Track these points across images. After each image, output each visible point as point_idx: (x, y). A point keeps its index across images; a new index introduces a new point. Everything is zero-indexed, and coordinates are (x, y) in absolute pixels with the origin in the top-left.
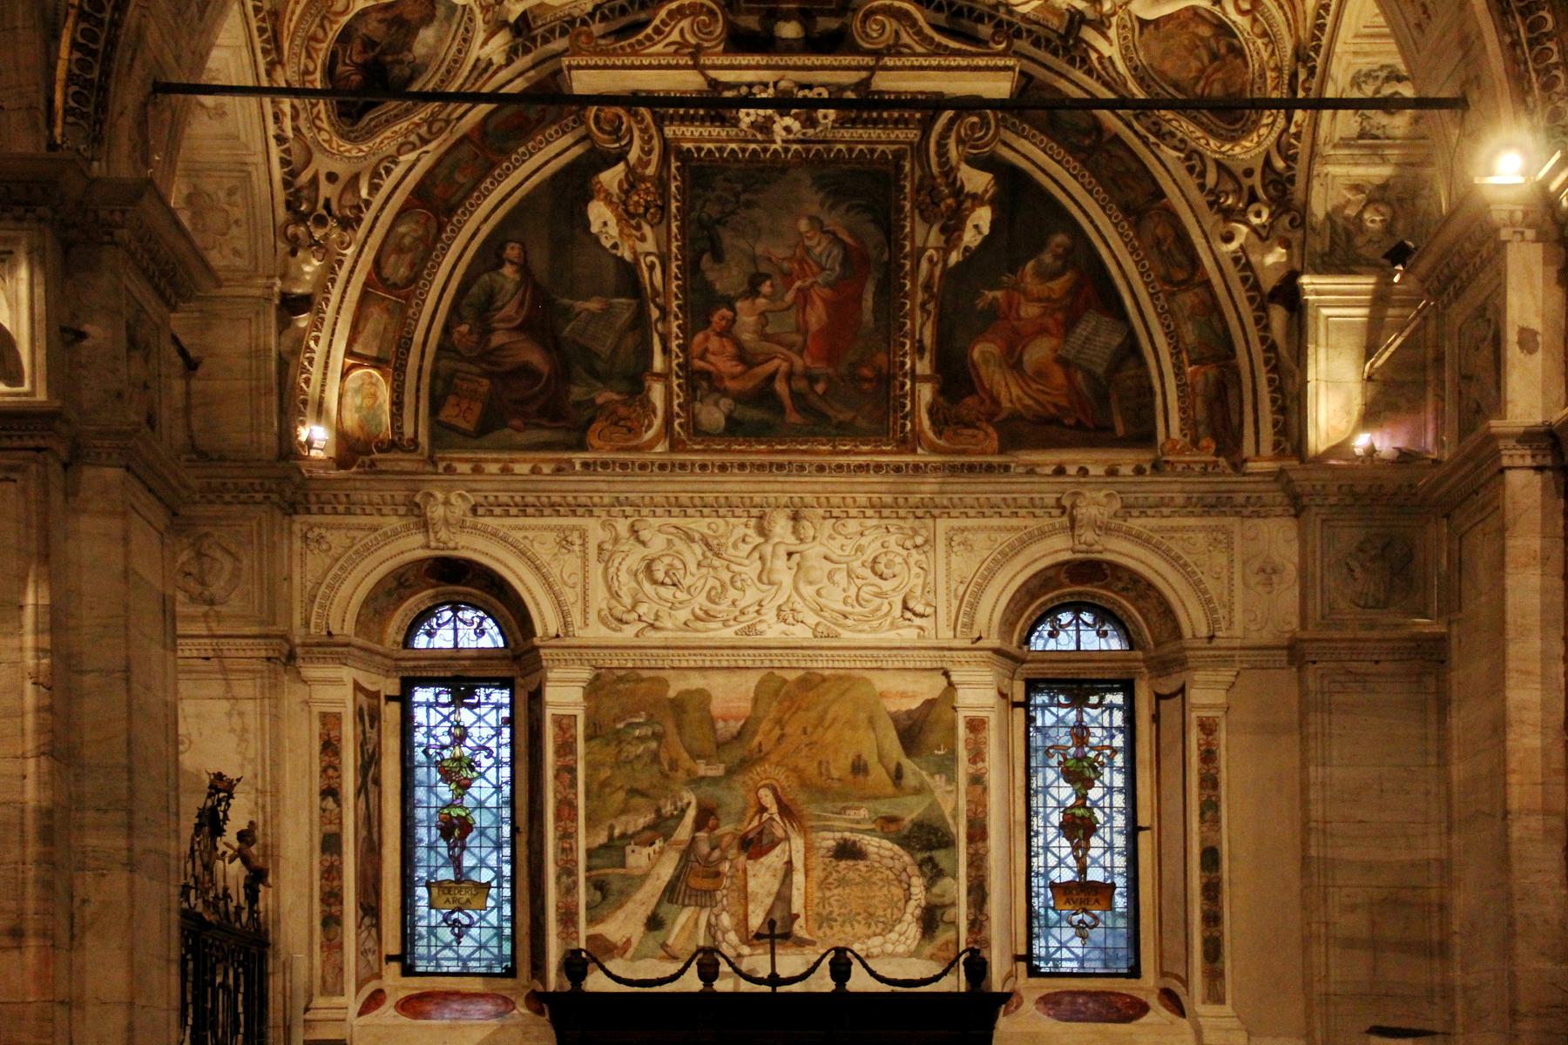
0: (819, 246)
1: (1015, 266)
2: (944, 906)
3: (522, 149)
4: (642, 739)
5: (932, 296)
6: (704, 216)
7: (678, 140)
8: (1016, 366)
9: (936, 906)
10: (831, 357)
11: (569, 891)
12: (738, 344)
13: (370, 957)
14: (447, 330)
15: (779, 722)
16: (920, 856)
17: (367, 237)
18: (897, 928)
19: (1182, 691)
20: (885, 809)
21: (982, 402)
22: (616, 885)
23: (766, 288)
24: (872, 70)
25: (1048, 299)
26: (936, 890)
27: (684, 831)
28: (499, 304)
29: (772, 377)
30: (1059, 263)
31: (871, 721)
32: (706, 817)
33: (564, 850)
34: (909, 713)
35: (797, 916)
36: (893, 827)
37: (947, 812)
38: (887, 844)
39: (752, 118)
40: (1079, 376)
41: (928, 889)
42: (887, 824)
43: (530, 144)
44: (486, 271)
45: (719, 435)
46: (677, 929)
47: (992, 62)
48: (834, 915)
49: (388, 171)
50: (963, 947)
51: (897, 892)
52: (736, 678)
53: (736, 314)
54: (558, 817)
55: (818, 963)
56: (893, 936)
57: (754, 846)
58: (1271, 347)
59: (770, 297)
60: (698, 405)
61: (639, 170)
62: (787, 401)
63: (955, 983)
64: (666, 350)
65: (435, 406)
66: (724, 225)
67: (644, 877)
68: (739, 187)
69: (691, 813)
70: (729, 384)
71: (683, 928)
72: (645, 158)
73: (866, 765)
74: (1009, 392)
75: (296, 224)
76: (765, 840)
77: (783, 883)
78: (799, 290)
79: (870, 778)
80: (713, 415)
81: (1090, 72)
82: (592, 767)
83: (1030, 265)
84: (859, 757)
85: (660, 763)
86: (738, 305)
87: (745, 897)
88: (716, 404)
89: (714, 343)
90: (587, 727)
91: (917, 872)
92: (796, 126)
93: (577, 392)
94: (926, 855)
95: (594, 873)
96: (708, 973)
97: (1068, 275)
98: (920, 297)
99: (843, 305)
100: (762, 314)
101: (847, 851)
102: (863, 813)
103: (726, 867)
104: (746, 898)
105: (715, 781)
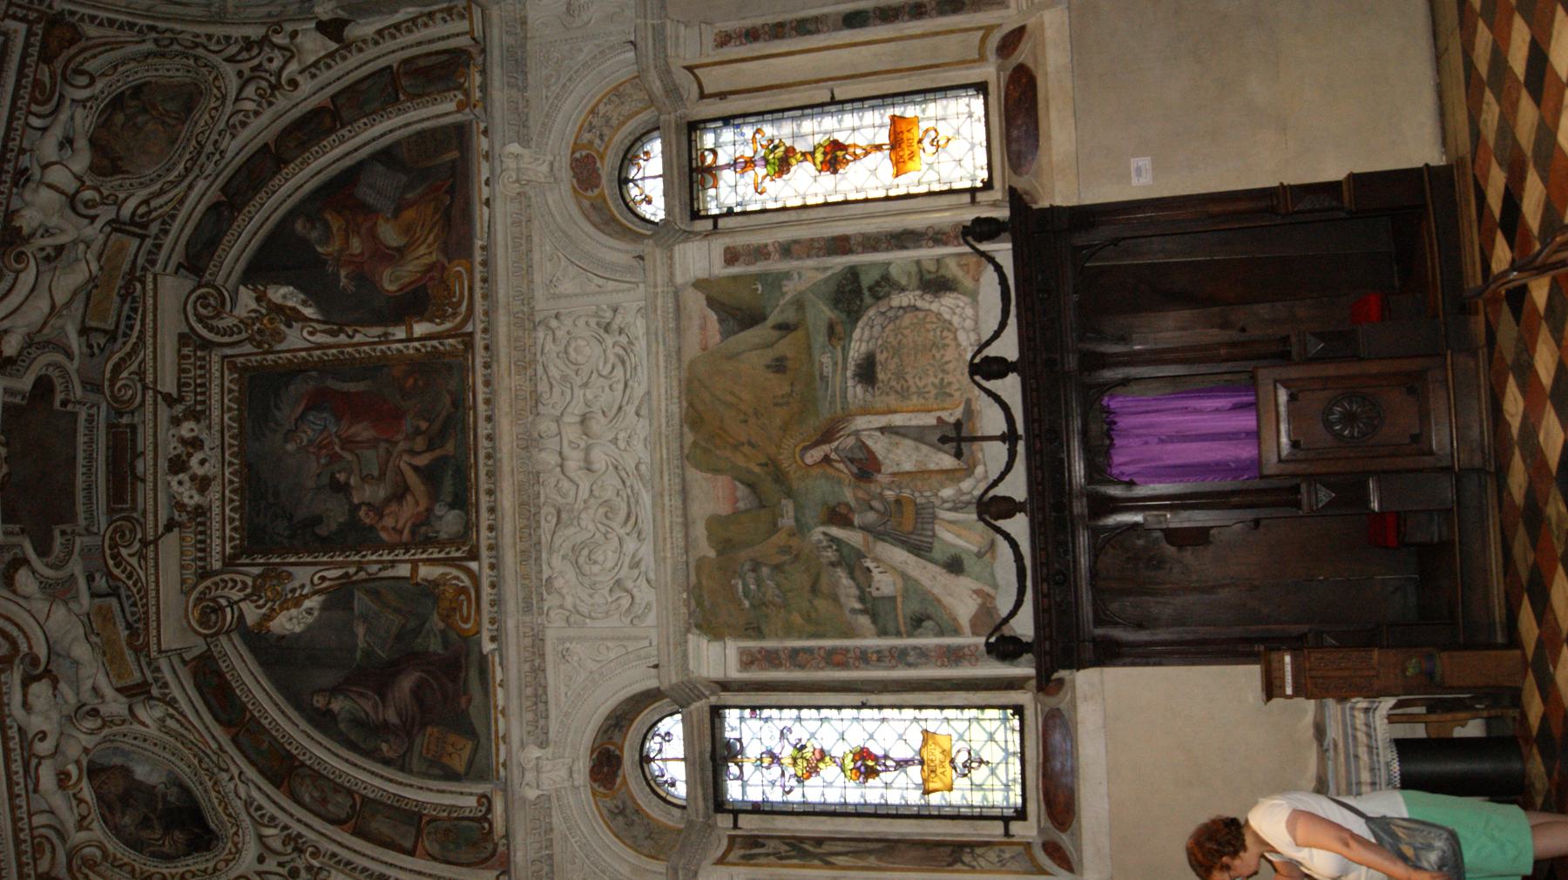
0: (307, 434)
1: (320, 262)
2: (920, 272)
3: (237, 691)
4: (759, 582)
5: (341, 331)
6: (286, 534)
8: (401, 251)
9: (921, 279)
10: (397, 416)
11: (924, 655)
12: (388, 501)
13: (1007, 856)
14: (387, 762)
15: (736, 447)
16: (868, 299)
17: (313, 830)
18: (947, 317)
19: (690, 69)
20: (820, 338)
21: (432, 278)
22: (915, 606)
23: (342, 477)
24: (156, 392)
26: (904, 282)
27: (854, 538)
29: (416, 469)
31: (730, 357)
32: (839, 516)
33: (879, 660)
34: (721, 321)
35: (939, 419)
36: (839, 329)
37: (821, 276)
38: (857, 334)
39: (194, 493)
40: (409, 196)
41: (903, 290)
42: (836, 335)
43: (234, 685)
45: (467, 514)
46: (961, 542)
47: (150, 293)
48: (937, 381)
49: (260, 808)
50: (967, 249)
51: (907, 319)
52: (695, 491)
53: (363, 503)
54: (843, 665)
55: (989, 393)
56: (956, 320)
57: (866, 467)
58: (380, 32)
60: (443, 536)
61: (249, 591)
62: (438, 453)
63: (1003, 250)
64: (393, 563)
65: (451, 776)
66: (292, 516)
67: (905, 576)
69: (835, 531)
70: (421, 508)
71: (959, 536)
72: (239, 586)
73: (777, 360)
74: (424, 255)
76: (860, 455)
77: (904, 436)
78: (342, 449)
79: (789, 354)
80: (449, 522)
81: (173, 217)
82: (789, 631)
83: (320, 249)
84: (768, 367)
85: (784, 563)
86: (356, 501)
87: (923, 473)
88: (440, 518)
89: (389, 522)
90: (749, 637)
91: (885, 301)
92: (198, 456)
93: (435, 645)
94: (866, 293)
95: (903, 629)
96: (1007, 507)
98: (342, 338)
99: (349, 407)
101: (867, 372)
102: (826, 359)
103: (890, 494)
104: (923, 472)
105: (799, 508)
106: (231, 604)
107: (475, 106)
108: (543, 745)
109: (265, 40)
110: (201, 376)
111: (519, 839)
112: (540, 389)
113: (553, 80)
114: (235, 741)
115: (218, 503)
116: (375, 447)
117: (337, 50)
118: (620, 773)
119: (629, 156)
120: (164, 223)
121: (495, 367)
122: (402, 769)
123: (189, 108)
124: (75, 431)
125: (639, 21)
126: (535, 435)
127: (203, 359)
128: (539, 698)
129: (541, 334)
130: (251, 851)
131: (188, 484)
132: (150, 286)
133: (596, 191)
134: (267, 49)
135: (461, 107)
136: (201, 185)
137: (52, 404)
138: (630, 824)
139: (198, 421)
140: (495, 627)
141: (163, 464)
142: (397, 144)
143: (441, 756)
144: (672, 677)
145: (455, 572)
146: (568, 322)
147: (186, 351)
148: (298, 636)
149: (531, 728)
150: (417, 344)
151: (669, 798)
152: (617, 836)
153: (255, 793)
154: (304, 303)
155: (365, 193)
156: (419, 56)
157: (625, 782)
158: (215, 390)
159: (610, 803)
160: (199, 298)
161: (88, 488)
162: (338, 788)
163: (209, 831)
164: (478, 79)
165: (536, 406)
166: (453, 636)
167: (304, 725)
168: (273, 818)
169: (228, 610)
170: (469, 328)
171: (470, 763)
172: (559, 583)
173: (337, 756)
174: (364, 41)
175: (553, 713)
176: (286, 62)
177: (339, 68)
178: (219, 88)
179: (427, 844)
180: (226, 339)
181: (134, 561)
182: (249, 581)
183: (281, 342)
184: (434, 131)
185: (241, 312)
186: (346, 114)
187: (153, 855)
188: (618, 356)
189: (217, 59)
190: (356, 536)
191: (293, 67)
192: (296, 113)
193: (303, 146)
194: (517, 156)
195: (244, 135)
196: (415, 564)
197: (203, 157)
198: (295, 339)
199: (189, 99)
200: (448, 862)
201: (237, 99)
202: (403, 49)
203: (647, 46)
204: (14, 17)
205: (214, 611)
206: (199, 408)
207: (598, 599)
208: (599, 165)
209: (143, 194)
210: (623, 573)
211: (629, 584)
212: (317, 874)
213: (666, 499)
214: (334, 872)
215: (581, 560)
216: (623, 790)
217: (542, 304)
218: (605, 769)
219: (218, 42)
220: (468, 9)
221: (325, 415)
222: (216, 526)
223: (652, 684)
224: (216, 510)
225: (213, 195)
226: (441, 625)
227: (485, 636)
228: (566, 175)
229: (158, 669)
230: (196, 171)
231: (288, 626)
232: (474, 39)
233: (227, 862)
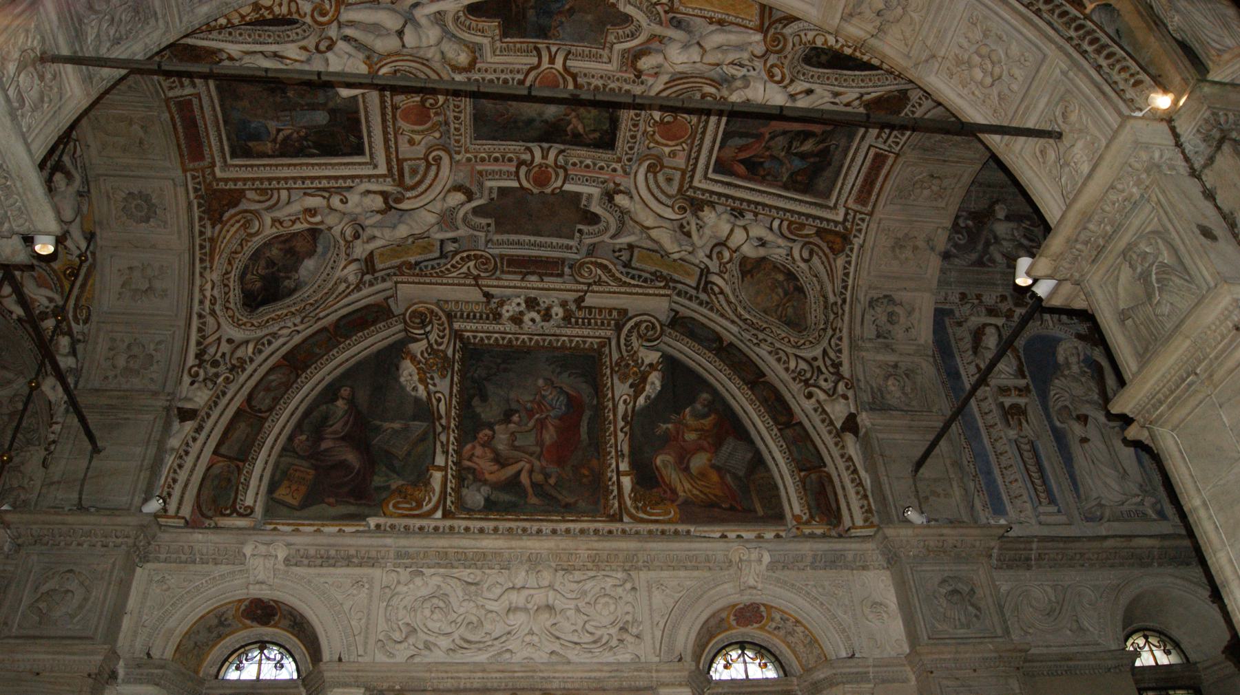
0: (550, 395)
1: (678, 410)
3: (361, 334)
5: (627, 423)
6: (476, 375)
7: (463, 331)
8: (687, 469)
10: (560, 462)
14: (291, 438)
17: (246, 381)
21: (665, 492)
23: (515, 418)
24: (586, 292)
25: (702, 430)
28: (331, 423)
29: (519, 472)
30: (706, 409)
39: (511, 313)
40: (729, 478)
43: (365, 332)
44: (326, 403)
45: (480, 511)
47: (657, 292)
49: (270, 343)
58: (850, 459)
59: (518, 424)
60: (464, 491)
61: (435, 347)
64: (446, 452)
65: (273, 487)
68: (499, 361)
70: (487, 476)
72: (440, 340)
74: (683, 487)
75: (199, 366)
78: (537, 420)
80: (475, 496)
81: (711, 309)
83: (688, 410)
86: (496, 427)
88: (479, 490)
89: (479, 451)
92: (538, 318)
93: (378, 481)
97: (713, 416)
99: (568, 426)
100: (513, 433)
106: (426, 334)
107: (798, 529)
108: (287, 561)
109: (841, 377)
110: (596, 324)
111: (213, 537)
112: (577, 573)
113: (820, 590)
114: (324, 329)
115: (502, 329)
116: (537, 445)
117: (835, 427)
118: (255, 624)
119: (763, 651)
120: (707, 303)
121: (595, 538)
122: (284, 449)
123: (789, 323)
124: (560, 237)
125: (871, 660)
126: (539, 568)
127: (609, 324)
128: (326, 560)
129: (620, 575)
130: (238, 335)
131: (517, 309)
132: (662, 292)
133: (734, 623)
134: (833, 378)
135: (797, 518)
136: (734, 329)
137: (580, 223)
138: (210, 630)
139: (564, 319)
140: (388, 529)
141: (533, 294)
142: (768, 470)
143: (289, 479)
144: (329, 672)
145: (435, 500)
146: (629, 598)
147: (615, 313)
148: (397, 379)
149: (301, 553)
150: (615, 479)
151: (227, 664)
152: (202, 617)
153: (281, 341)
154: (648, 397)
155: (730, 445)
156: (834, 487)
157: (246, 627)
158: (586, 332)
159: (230, 614)
160: (653, 324)
161: (518, 243)
162: (276, 400)
163: (257, 307)
164: (819, 531)
165: (563, 570)
166: (384, 495)
167: (328, 379)
168: (260, 352)
169: (422, 332)
170: (626, 519)
171: (284, 504)
172: (418, 581)
173: (301, 402)
174: (843, 447)
175: (312, 571)
176: (824, 391)
177: (823, 429)
178: (804, 344)
179: (221, 464)
180: (622, 341)
181: (464, 270)
182: (442, 347)
183: (619, 379)
184: (778, 497)
185: (642, 353)
186: (789, 432)
187: (246, 267)
188: (601, 638)
189: (825, 343)
190: (470, 426)
191: (822, 396)
192: (788, 397)
193: (764, 402)
194: (760, 561)
195: (771, 360)
196: (444, 469)
197: (755, 332)
198: (622, 390)
199: (796, 323)
200: (203, 479)
201: (797, 356)
202: (839, 475)
203: (851, 667)
204: (847, 214)
205: (423, 322)
206: (573, 320)
207: (402, 613)
208: (756, 625)
209: (727, 290)
210: (421, 635)
211: (411, 640)
212: (212, 381)
213: (480, 675)
214: (211, 393)
215: (435, 601)
216: (240, 625)
217: (643, 577)
218: (259, 612)
219: (837, 345)
220: (872, 525)
221: (563, 408)
222: (486, 327)
223: (326, 656)
224: (497, 327)
225: (728, 338)
226: (394, 487)
227: (381, 520)
228: (746, 599)
229: (384, 280)
230: (745, 326)
231: (405, 373)
232: (849, 529)
233: (232, 317)
